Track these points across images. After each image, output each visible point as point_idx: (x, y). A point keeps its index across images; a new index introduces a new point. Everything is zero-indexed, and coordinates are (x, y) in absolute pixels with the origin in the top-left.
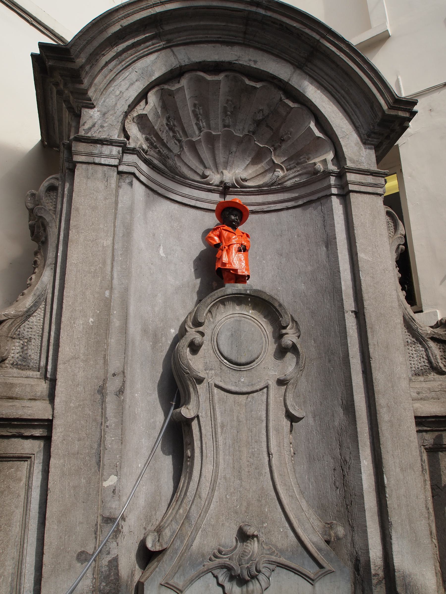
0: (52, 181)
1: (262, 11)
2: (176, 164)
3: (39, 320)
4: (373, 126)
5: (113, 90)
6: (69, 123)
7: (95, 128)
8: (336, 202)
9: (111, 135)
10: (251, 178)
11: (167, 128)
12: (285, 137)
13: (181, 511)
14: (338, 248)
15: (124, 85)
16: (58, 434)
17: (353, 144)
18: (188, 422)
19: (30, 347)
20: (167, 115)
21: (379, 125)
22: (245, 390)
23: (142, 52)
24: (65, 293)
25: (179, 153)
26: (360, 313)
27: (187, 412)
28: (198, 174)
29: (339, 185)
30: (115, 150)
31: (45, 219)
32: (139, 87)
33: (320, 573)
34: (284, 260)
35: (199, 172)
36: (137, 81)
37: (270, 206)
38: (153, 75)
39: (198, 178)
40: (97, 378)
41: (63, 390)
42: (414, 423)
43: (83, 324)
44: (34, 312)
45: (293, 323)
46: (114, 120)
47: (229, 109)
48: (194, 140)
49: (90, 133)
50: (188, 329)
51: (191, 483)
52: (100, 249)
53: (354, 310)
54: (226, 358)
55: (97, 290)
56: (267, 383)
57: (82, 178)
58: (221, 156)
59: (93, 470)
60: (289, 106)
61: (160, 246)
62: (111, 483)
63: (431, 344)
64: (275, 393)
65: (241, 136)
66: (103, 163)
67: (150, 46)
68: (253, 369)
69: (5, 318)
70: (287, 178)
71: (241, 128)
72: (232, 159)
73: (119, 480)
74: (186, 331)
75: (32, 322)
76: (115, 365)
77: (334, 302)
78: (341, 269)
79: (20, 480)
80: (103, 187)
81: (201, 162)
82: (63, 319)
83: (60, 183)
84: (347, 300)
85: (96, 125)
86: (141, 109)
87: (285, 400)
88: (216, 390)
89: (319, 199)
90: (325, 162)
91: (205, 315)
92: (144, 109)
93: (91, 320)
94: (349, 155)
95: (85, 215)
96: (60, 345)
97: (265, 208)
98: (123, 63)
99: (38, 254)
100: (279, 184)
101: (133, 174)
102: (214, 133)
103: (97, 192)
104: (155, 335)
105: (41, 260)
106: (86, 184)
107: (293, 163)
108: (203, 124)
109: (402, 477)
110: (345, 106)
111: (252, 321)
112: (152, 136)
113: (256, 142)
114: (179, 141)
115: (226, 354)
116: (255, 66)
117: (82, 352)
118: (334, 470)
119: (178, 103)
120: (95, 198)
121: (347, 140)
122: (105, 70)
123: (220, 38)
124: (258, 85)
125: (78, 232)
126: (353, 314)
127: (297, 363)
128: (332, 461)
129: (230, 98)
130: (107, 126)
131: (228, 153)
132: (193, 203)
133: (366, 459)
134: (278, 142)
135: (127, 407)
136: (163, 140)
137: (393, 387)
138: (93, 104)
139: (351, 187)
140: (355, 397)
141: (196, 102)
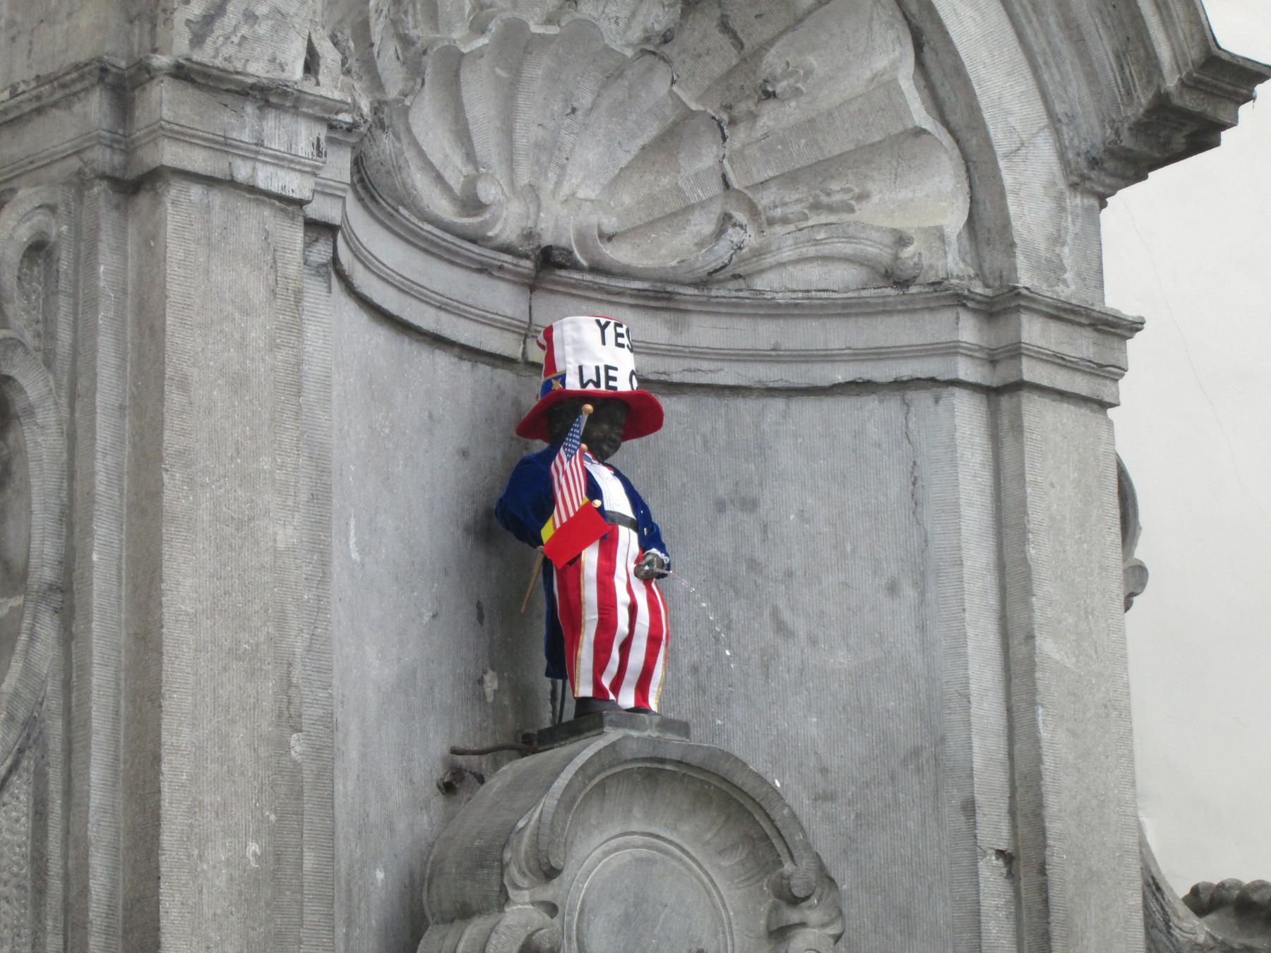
3: (17, 821)
4: (1117, 133)
7: (226, 19)
8: (966, 414)
10: (629, 231)
12: (779, 88)
14: (967, 606)
17: (1037, 187)
29: (981, 348)
31: (21, 390)
35: (452, 183)
37: (693, 364)
39: (443, 208)
43: (228, 863)
50: (512, 893)
52: (267, 559)
53: (1003, 847)
57: (192, 246)
65: (629, 53)
66: (262, 184)
71: (624, 13)
72: (571, 138)
78: (973, 687)
81: (463, 135)
83: (64, 228)
84: (986, 810)
89: (900, 385)
93: (253, 847)
94: (1025, 234)
95: (209, 412)
96: (163, 940)
100: (736, 277)
103: (245, 312)
106: (208, 272)
107: (799, 201)
110: (1024, 21)
111: (684, 864)
121: (1022, 166)
126: (1000, 863)
130: (267, 17)
131: (557, 107)
132: (425, 318)
139: (1031, 371)
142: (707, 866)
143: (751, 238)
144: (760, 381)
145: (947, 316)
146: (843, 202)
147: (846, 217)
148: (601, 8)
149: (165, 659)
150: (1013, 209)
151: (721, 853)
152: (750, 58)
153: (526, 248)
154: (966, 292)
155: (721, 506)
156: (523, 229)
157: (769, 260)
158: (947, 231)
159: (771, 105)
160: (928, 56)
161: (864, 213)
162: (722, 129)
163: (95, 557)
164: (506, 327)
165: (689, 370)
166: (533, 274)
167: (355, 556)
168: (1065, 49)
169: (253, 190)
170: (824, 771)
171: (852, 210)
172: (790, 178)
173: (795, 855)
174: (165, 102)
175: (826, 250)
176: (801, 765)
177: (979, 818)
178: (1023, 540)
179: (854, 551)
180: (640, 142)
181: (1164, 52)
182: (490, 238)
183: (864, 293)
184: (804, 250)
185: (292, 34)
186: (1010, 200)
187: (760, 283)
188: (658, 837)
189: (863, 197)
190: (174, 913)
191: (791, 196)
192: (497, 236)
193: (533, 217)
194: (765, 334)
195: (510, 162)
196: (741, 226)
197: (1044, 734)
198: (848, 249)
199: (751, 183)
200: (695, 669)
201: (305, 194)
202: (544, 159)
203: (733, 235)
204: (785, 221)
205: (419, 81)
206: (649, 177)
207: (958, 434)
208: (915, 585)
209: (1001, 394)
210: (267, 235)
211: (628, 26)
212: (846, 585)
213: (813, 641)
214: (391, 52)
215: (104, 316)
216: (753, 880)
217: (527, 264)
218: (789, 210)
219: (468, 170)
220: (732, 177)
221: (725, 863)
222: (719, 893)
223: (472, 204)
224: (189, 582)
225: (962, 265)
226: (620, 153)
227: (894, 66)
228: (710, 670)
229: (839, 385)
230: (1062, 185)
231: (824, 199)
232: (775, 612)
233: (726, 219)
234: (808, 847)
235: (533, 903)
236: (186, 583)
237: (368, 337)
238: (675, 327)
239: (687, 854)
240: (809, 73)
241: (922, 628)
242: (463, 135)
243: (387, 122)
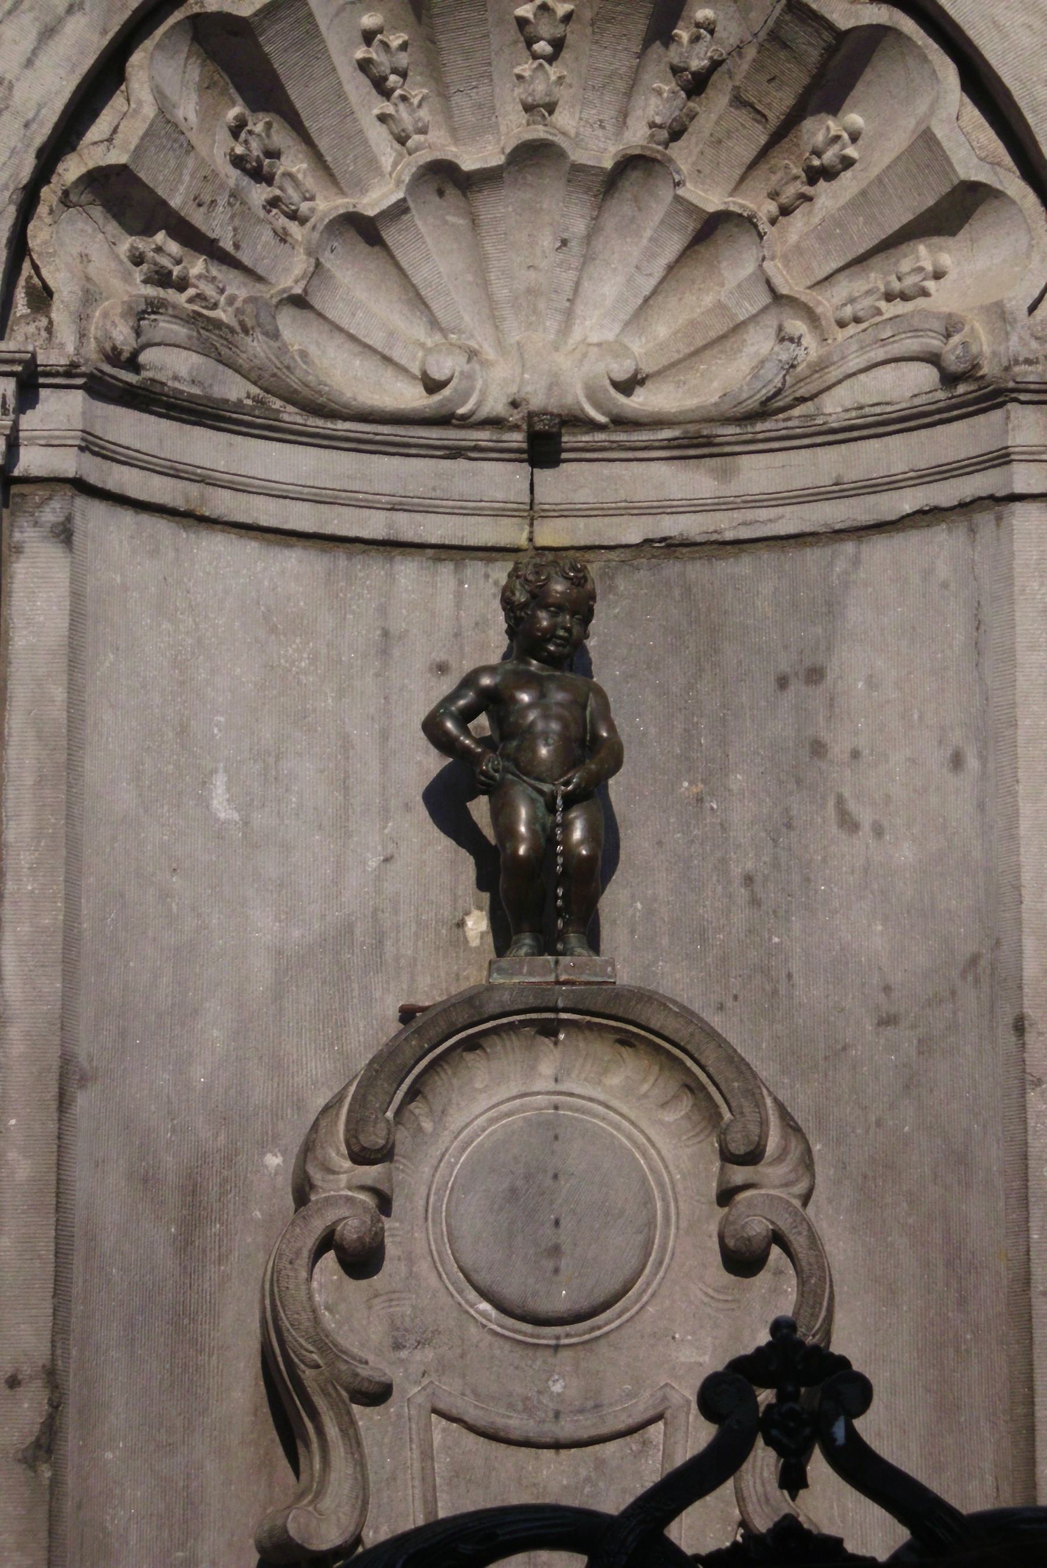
2: (284, 349)
11: (233, 176)
22: (567, 1429)
25: (298, 290)
35: (403, 362)
36: (70, 10)
37: (750, 515)
45: (785, 1137)
54: (485, 1294)
56: (664, 1399)
60: (830, 26)
61: (215, 771)
68: (603, 1341)
70: (834, 374)
71: (609, 114)
78: (1027, 876)
81: (417, 300)
88: (440, 1430)
89: (966, 507)
91: (390, 1114)
92: (110, 140)
97: (728, 525)
104: (192, 1190)
107: (869, 293)
113: (680, 192)
115: (483, 1278)
131: (547, 241)
132: (373, 525)
134: (796, 178)
135: (69, 1506)
136: (214, 241)
142: (644, 1124)
144: (826, 525)
145: (997, 415)
146: (915, 285)
147: (921, 302)
148: (577, 116)
151: (663, 1105)
153: (515, 417)
154: (1011, 385)
155: (782, 682)
156: (508, 396)
158: (1009, 306)
162: (756, 226)
164: (498, 514)
165: (744, 524)
166: (525, 445)
170: (887, 989)
171: (925, 293)
173: (733, 1105)
176: (863, 985)
177: (1030, 1037)
179: (921, 718)
182: (463, 417)
183: (917, 401)
184: (872, 354)
188: (571, 1095)
192: (472, 413)
193: (518, 379)
195: (495, 320)
196: (791, 340)
198: (912, 345)
199: (814, 280)
200: (749, 880)
202: (542, 305)
204: (857, 320)
205: (313, 261)
206: (690, 298)
207: (1018, 562)
212: (913, 761)
213: (878, 831)
214: (267, 235)
216: (702, 1137)
217: (517, 439)
218: (858, 306)
219: (431, 340)
220: (778, 282)
221: (670, 1117)
222: (659, 1153)
225: (1034, 345)
226: (640, 279)
228: (766, 878)
229: (908, 515)
231: (896, 286)
232: (840, 800)
235: (350, 1189)
237: (260, 565)
238: (725, 475)
239: (615, 1111)
240: (855, 137)
241: (981, 807)
243: (249, 323)
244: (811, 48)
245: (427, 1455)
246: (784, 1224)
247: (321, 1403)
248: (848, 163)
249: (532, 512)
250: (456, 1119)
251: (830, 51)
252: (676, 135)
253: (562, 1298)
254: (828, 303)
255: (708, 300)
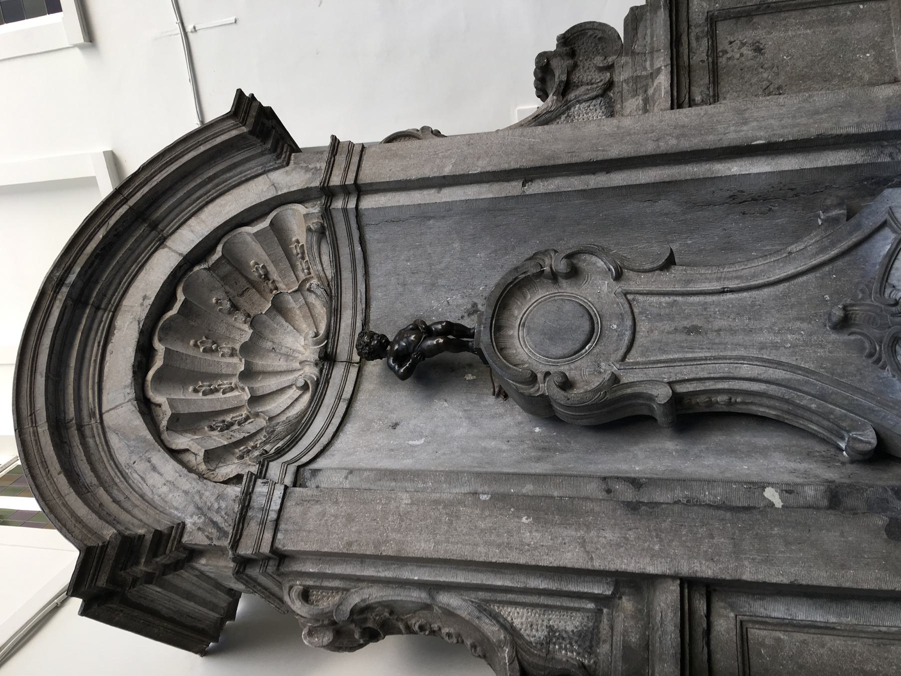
0: (293, 594)
1: (72, 278)
5: (160, 496)
6: (196, 576)
9: (234, 497)
13: (813, 406)
15: (154, 479)
16: (704, 568)
17: (289, 178)
18: (677, 400)
19: (563, 628)
20: (206, 429)
21: (264, 141)
22: (629, 323)
23: (102, 453)
24: (481, 559)
26: (527, 174)
27: (662, 394)
28: (300, 396)
30: (261, 488)
31: (356, 605)
32: (161, 459)
33: (893, 224)
34: (441, 282)
36: (149, 462)
37: (359, 300)
38: (145, 438)
39: (307, 397)
40: (614, 510)
41: (633, 561)
42: (681, 110)
43: (530, 532)
44: (505, 619)
46: (209, 492)
47: (209, 345)
48: (246, 396)
49: (226, 529)
51: (770, 392)
52: (414, 508)
53: (521, 184)
54: (583, 347)
55: (478, 511)
58: (276, 363)
59: (759, 517)
62: (777, 495)
63: (572, 96)
64: (636, 283)
65: (252, 331)
67: (95, 441)
69: (516, 662)
70: (322, 274)
73: (772, 485)
74: (542, 395)
75: (522, 624)
76: (593, 489)
77: (507, 210)
79: (778, 640)
80: (318, 506)
81: (282, 390)
82: (522, 561)
85: (215, 519)
86: (197, 460)
87: (645, 271)
89: (360, 228)
90: (306, 216)
93: (524, 520)
97: (361, 306)
98: (117, 480)
99: (409, 623)
100: (329, 285)
101: (299, 467)
102: (243, 369)
103: (324, 515)
105: (420, 618)
106: (309, 531)
108: (225, 384)
109: (755, 124)
112: (237, 451)
114: (247, 418)
115: (578, 346)
116: (153, 299)
117: (573, 533)
118: (744, 214)
119: (191, 411)
120: (333, 519)
122: (127, 505)
123: (99, 343)
124: (181, 297)
125: (386, 542)
127: (592, 253)
128: (731, 216)
129: (192, 342)
133: (729, 169)
137: (630, 134)
138: (179, 524)
139: (350, 180)
140: (643, 182)
141: (191, 389)
143: (315, 282)
145: (334, 213)
149: (452, 558)
150: (295, 188)
151: (525, 298)
152: (253, 284)
157: (322, 274)
159: (270, 277)
160: (246, 221)
161: (303, 241)
163: (416, 578)
164: (347, 371)
167: (422, 441)
168: (239, 170)
169: (280, 511)
172: (293, 267)
174: (246, 549)
175: (317, 255)
178: (410, 181)
180: (284, 322)
181: (234, 133)
185: (225, 492)
186: (292, 189)
187: (330, 278)
189: (298, 241)
190: (551, 559)
191: (300, 267)
194: (346, 275)
197: (479, 170)
198: (315, 247)
201: (282, 487)
203: (314, 287)
204: (308, 269)
208: (429, 220)
209: (359, 190)
210: (297, 504)
211: (243, 330)
215: (329, 570)
223: (305, 387)
224: (423, 545)
227: (249, 234)
230: (287, 168)
233: (309, 290)
234: (523, 265)
236: (422, 546)
240: (256, 263)
241: (444, 217)
242: (282, 390)
244: (227, 268)
245: (637, 363)
246: (563, 255)
247: (619, 393)
248: (264, 267)
249: (350, 362)
250: (525, 358)
251: (229, 263)
252: (249, 316)
253: (586, 326)
254: (302, 276)
255: (298, 312)
